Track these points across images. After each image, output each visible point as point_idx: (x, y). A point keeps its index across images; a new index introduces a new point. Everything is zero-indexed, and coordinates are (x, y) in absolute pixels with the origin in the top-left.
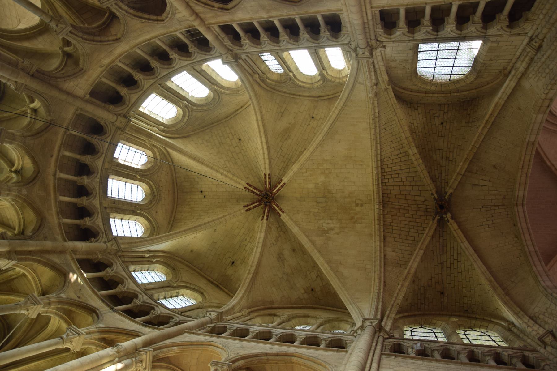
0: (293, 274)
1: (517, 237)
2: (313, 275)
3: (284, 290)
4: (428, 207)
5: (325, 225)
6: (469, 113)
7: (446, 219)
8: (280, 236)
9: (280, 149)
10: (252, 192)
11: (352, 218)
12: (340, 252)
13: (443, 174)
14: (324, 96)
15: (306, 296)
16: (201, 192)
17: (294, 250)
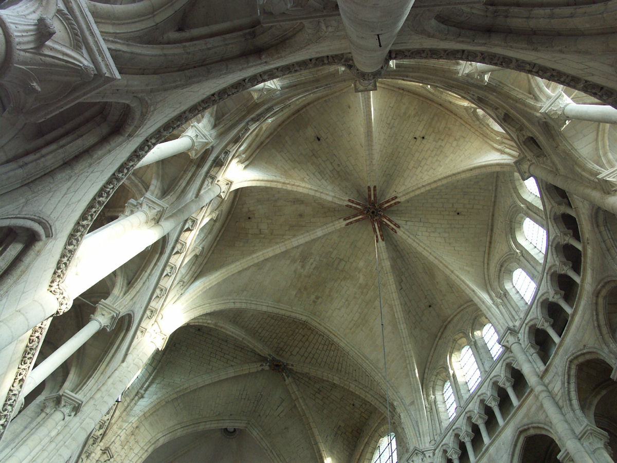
0: (274, 206)
1: (219, 414)
2: (264, 227)
3: (259, 195)
4: (285, 352)
5: (312, 261)
6: (347, 433)
7: (264, 364)
8: (323, 208)
9: (417, 257)
10: (388, 202)
11: (305, 289)
12: (273, 269)
13: (307, 380)
14: (442, 333)
15: (245, 210)
16: (423, 138)
17: (301, 215)
